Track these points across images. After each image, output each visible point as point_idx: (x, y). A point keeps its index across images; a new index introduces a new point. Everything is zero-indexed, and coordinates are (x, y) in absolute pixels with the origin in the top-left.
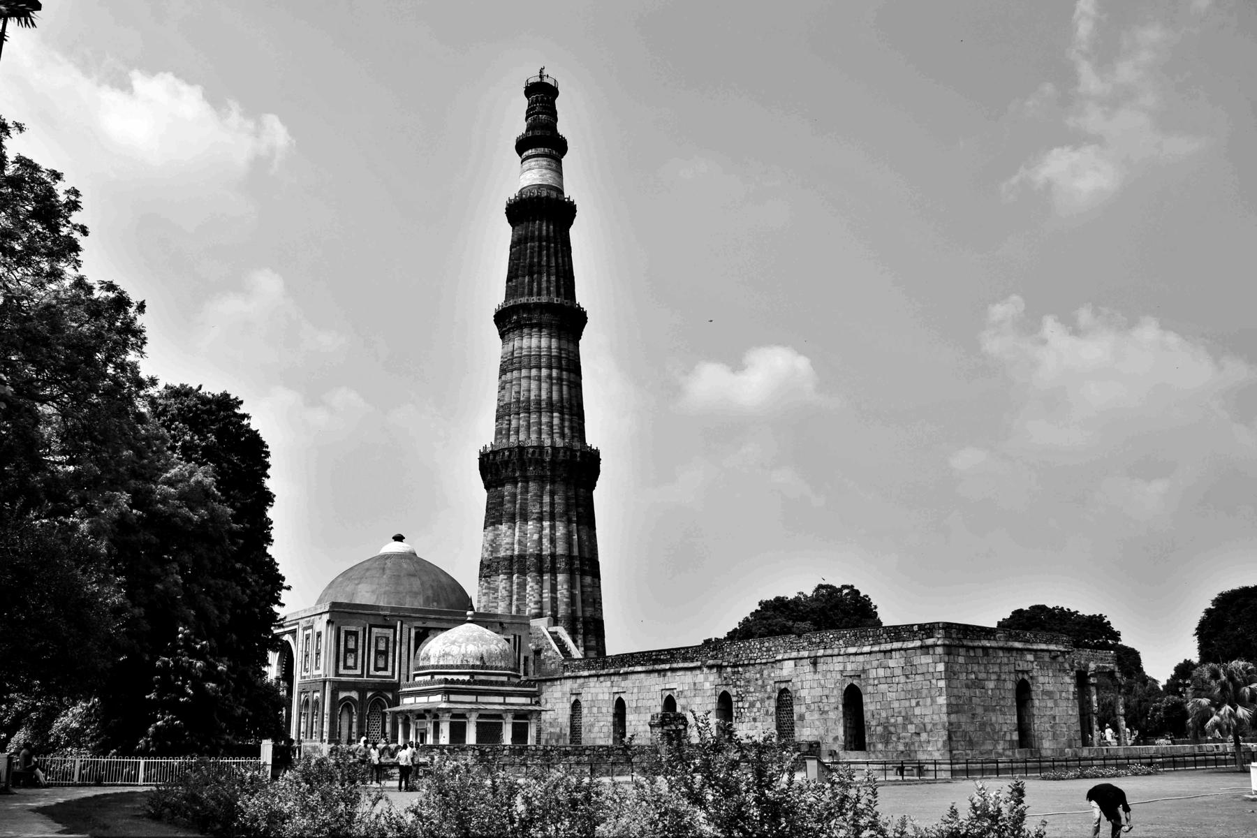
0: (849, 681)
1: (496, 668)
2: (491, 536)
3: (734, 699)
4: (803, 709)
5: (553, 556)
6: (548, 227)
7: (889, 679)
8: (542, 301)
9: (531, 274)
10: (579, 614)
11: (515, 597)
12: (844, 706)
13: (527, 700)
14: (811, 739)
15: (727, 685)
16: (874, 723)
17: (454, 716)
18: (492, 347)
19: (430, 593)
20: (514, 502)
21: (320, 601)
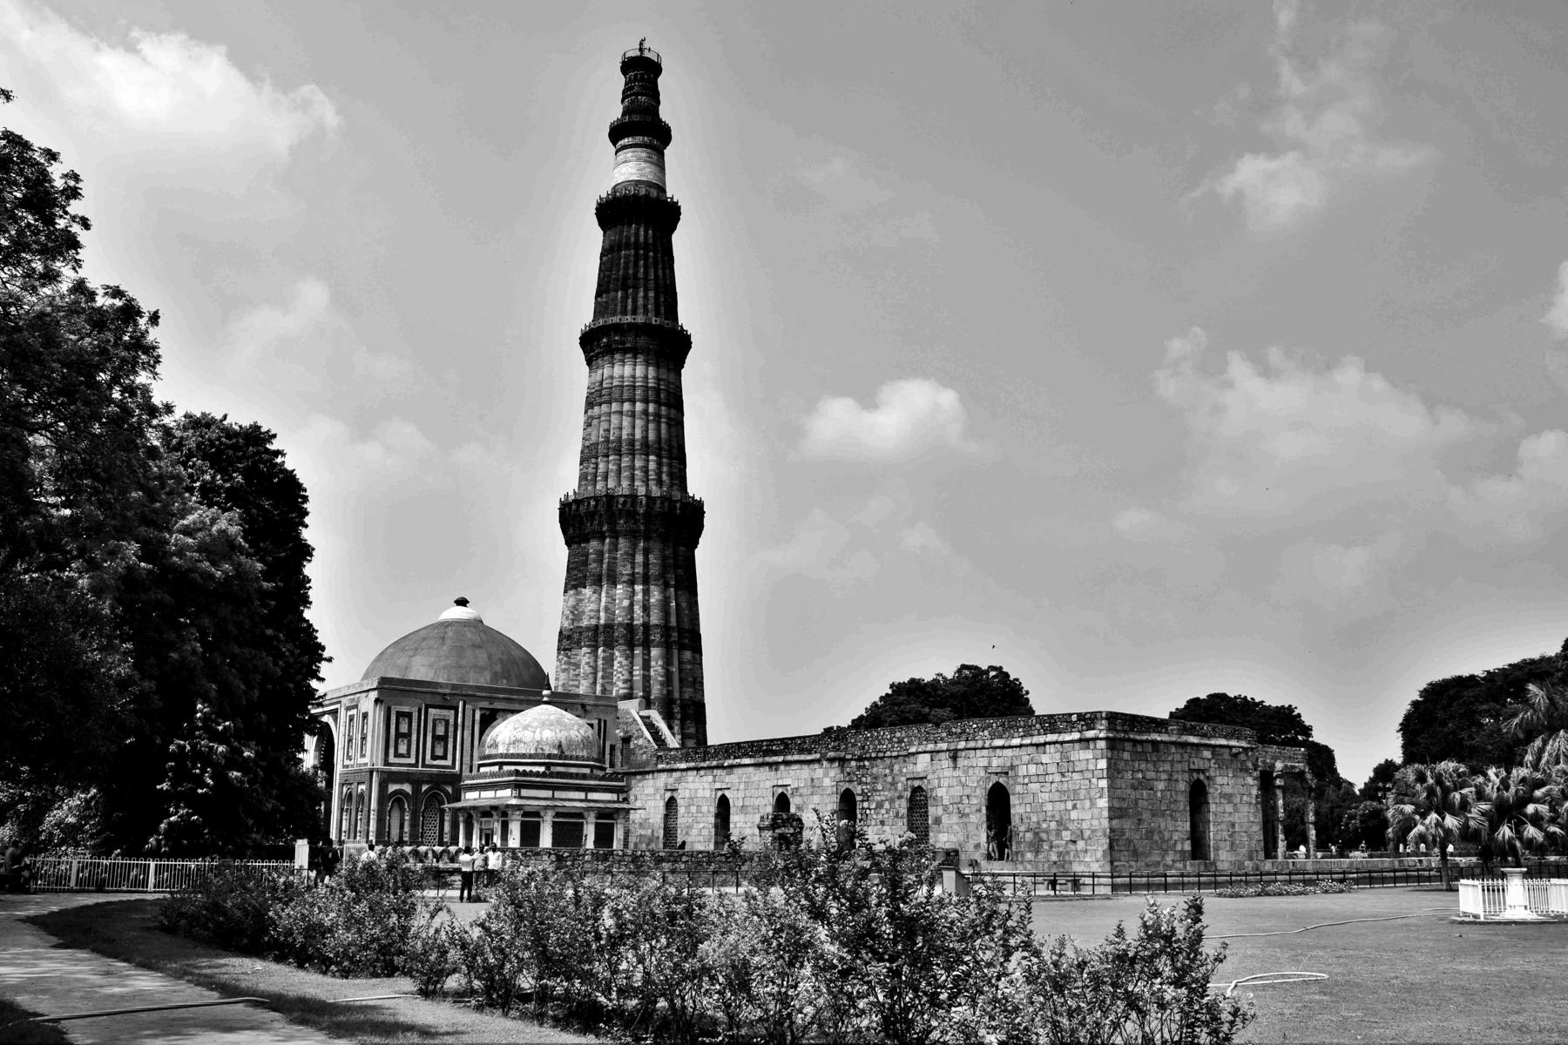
0: (994, 779)
1: (577, 758)
2: (572, 602)
3: (859, 798)
4: (940, 811)
5: (646, 626)
6: (646, 232)
7: (1041, 778)
8: (638, 321)
9: (625, 289)
11: (600, 674)
13: (613, 797)
14: (948, 846)
15: (851, 781)
16: (1022, 828)
17: (525, 814)
18: (577, 376)
19: (498, 668)
20: (601, 562)
21: (366, 676)
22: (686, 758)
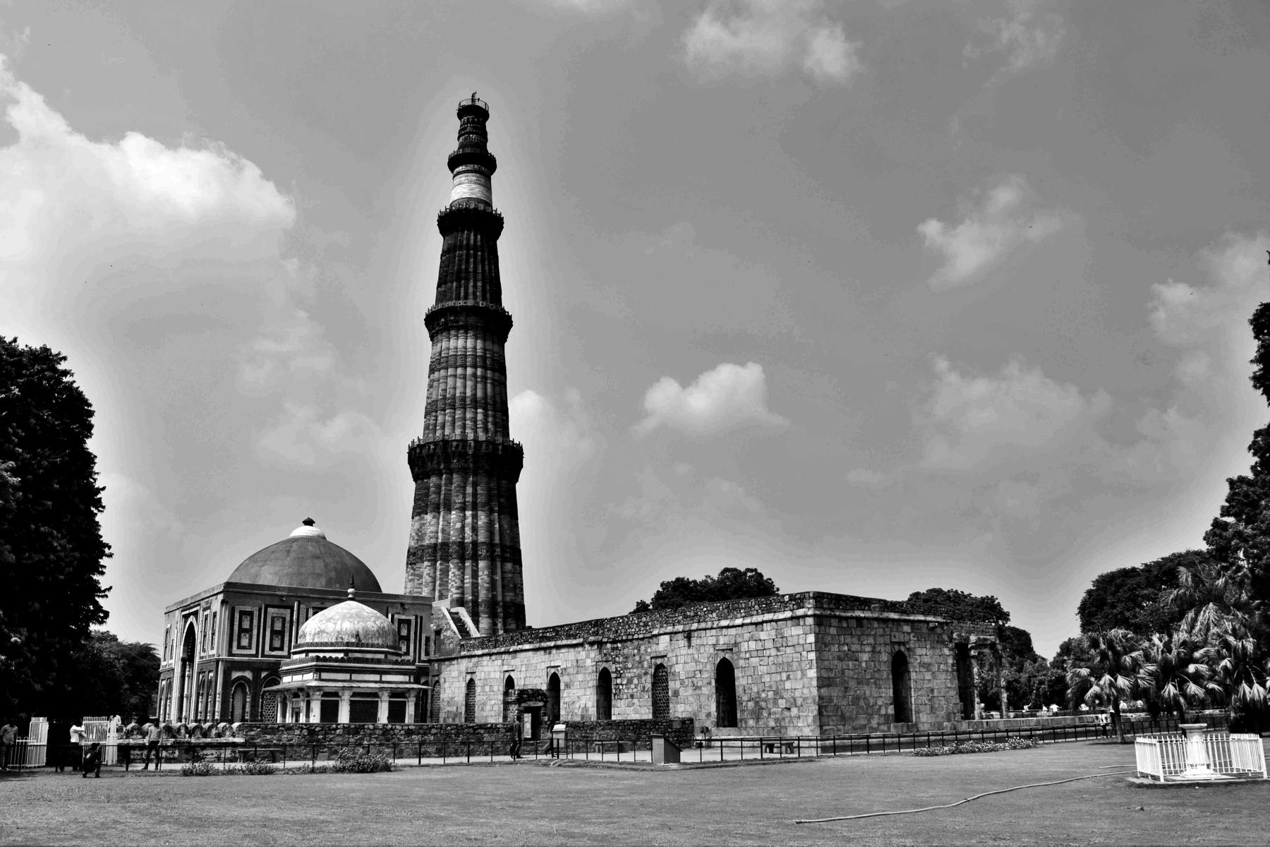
0: (721, 655)
1: (373, 646)
2: (417, 526)
3: (613, 675)
5: (475, 543)
6: (475, 236)
8: (470, 305)
9: (459, 281)
10: (500, 598)
12: (717, 681)
13: (406, 678)
14: (684, 715)
15: (607, 661)
16: (745, 698)
18: (423, 348)
19: (333, 574)
20: (439, 493)
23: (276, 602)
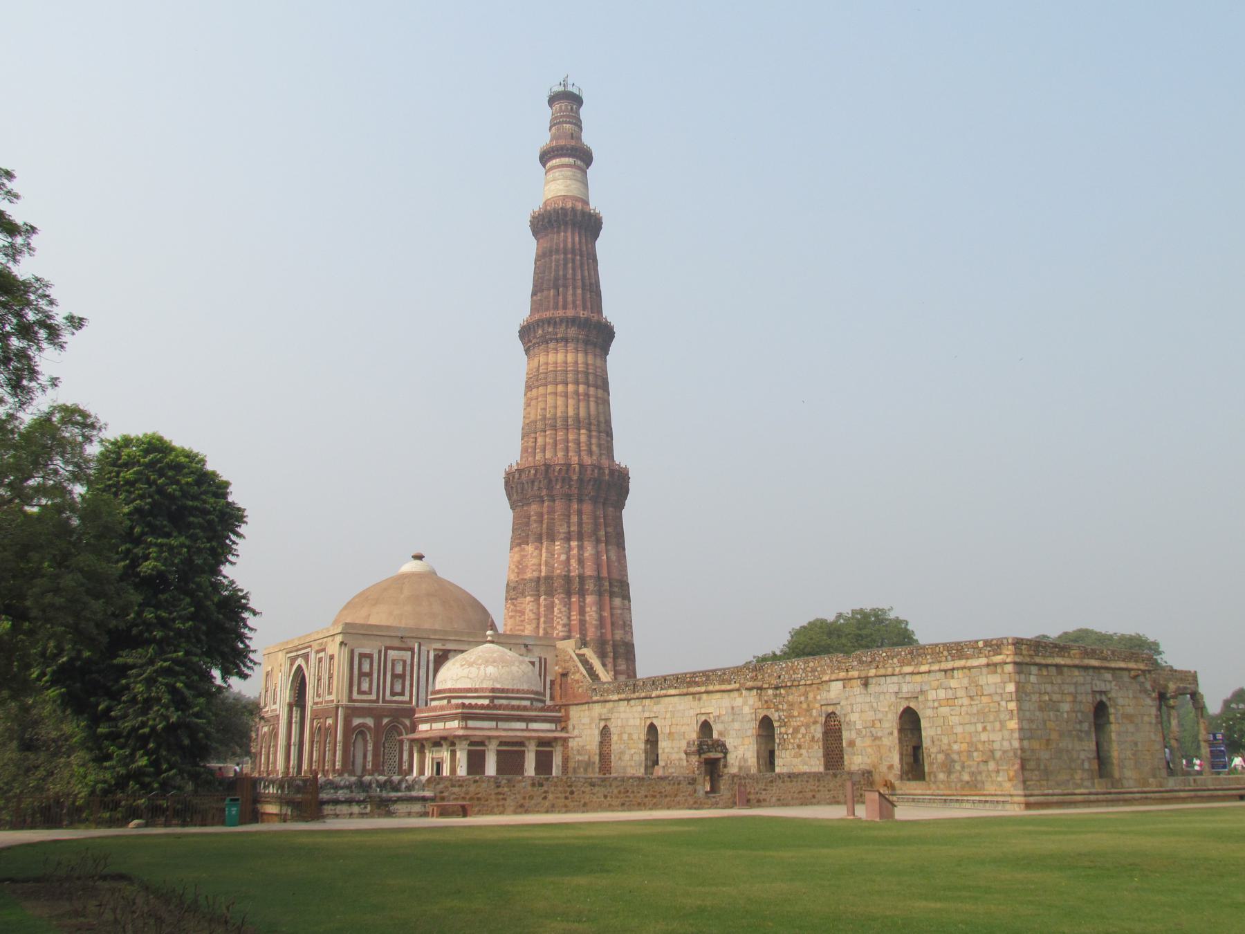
0: (904, 704)
1: (518, 691)
2: (517, 557)
3: (776, 724)
4: (854, 735)
5: (582, 578)
6: (573, 239)
7: (950, 702)
9: (556, 287)
11: (542, 620)
12: (901, 731)
13: (552, 726)
15: (768, 708)
17: (472, 744)
18: (516, 363)
20: (541, 522)
21: (336, 622)
22: (618, 690)
23: (397, 643)
